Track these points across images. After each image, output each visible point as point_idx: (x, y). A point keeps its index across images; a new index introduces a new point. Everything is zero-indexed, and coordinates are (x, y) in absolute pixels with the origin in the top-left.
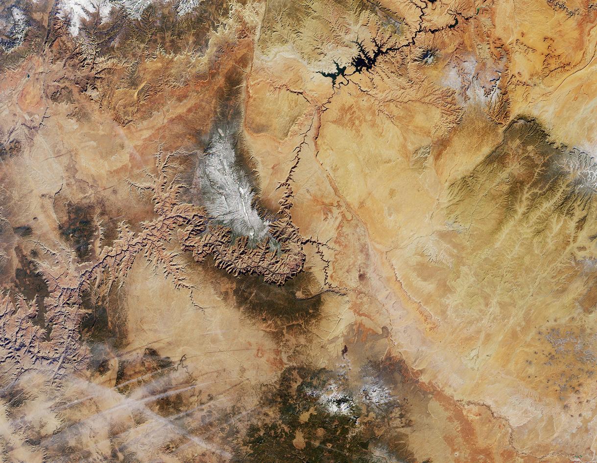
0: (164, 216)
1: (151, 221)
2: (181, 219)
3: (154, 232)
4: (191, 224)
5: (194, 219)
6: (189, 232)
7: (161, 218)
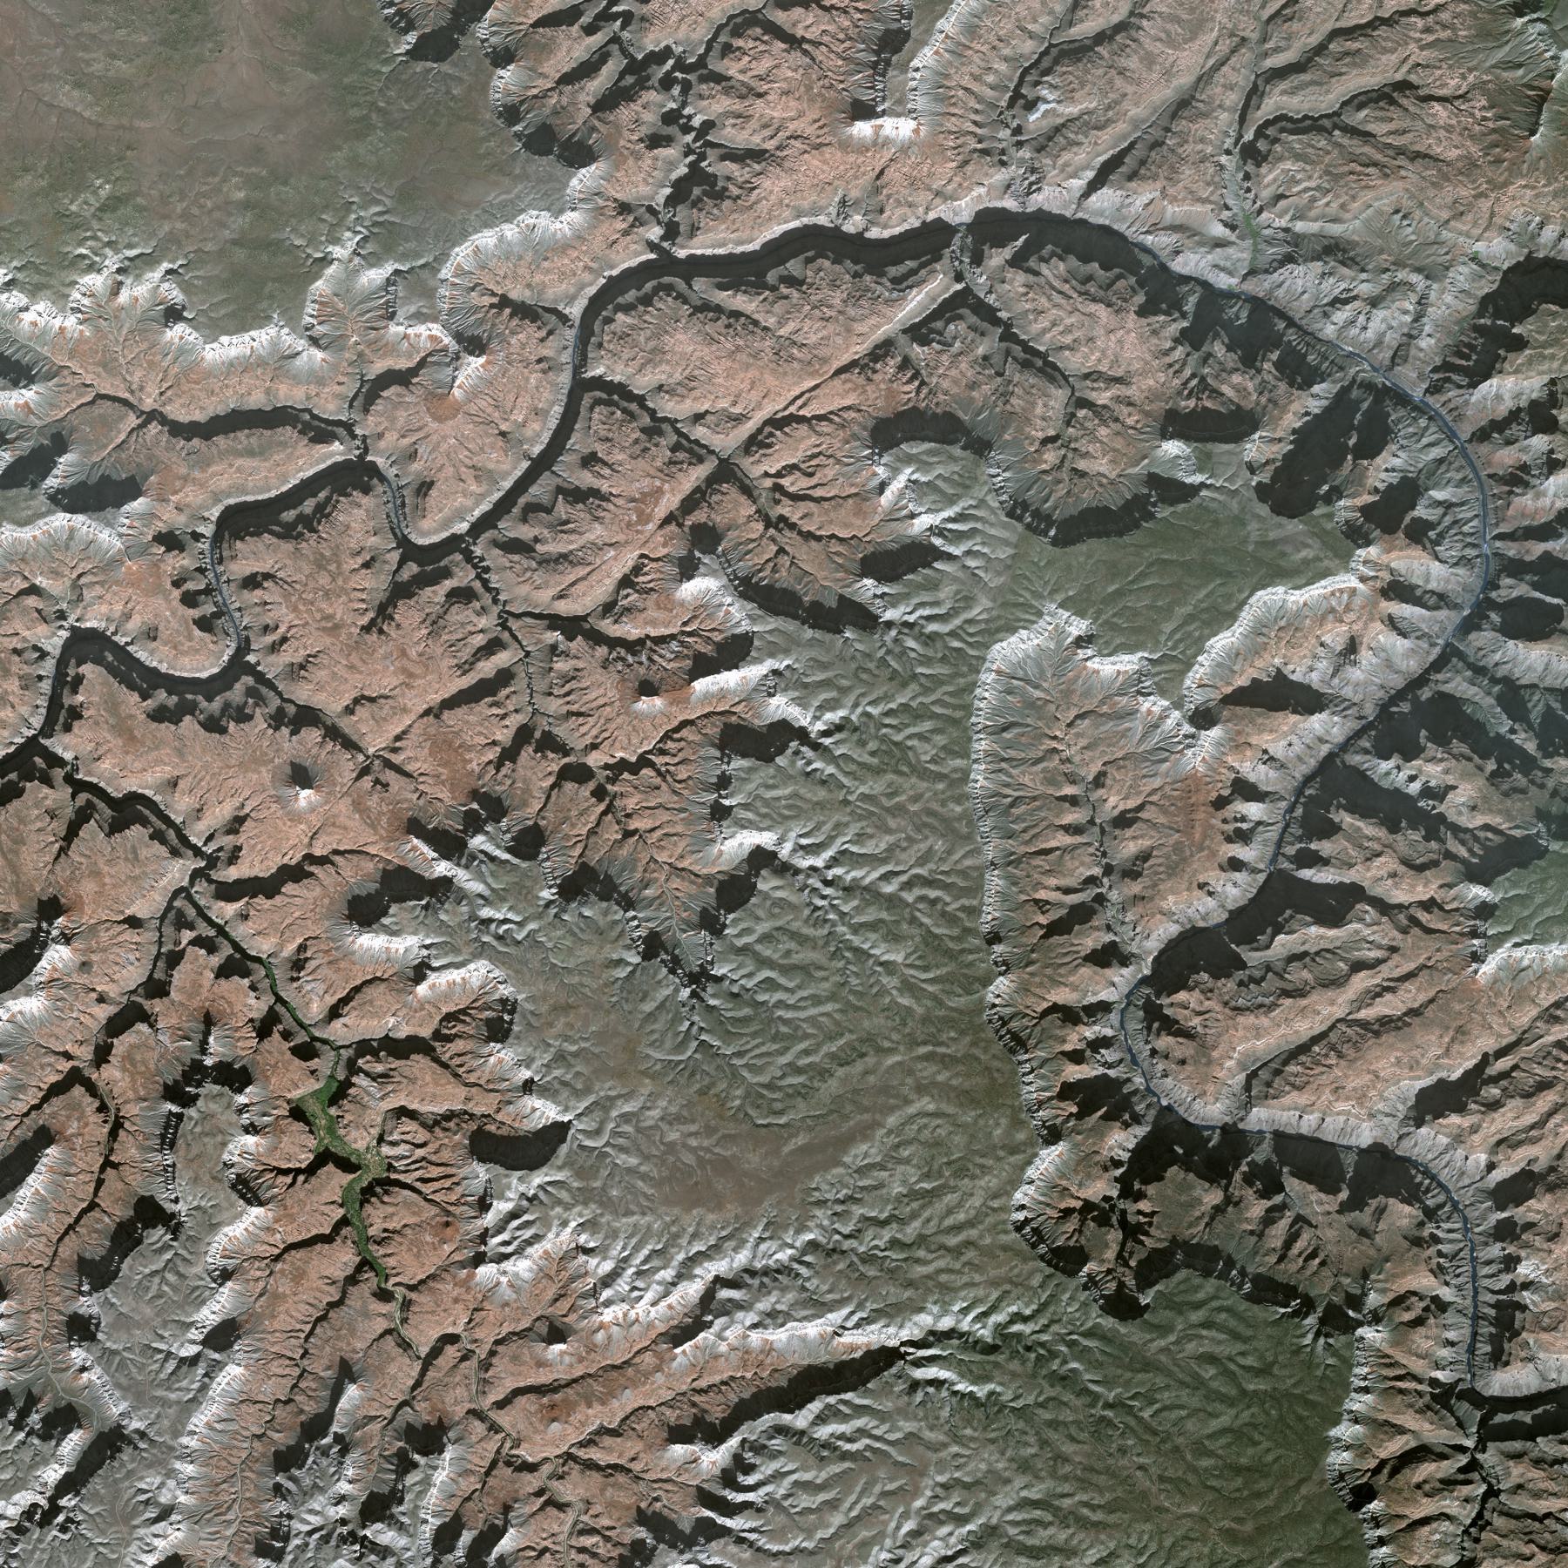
0: (650, 178)
1: (255, 280)
2: (1123, 347)
3: (309, 604)
4: (1391, 514)
5: (1508, 388)
6: (1298, 739)
7: (554, 234)
